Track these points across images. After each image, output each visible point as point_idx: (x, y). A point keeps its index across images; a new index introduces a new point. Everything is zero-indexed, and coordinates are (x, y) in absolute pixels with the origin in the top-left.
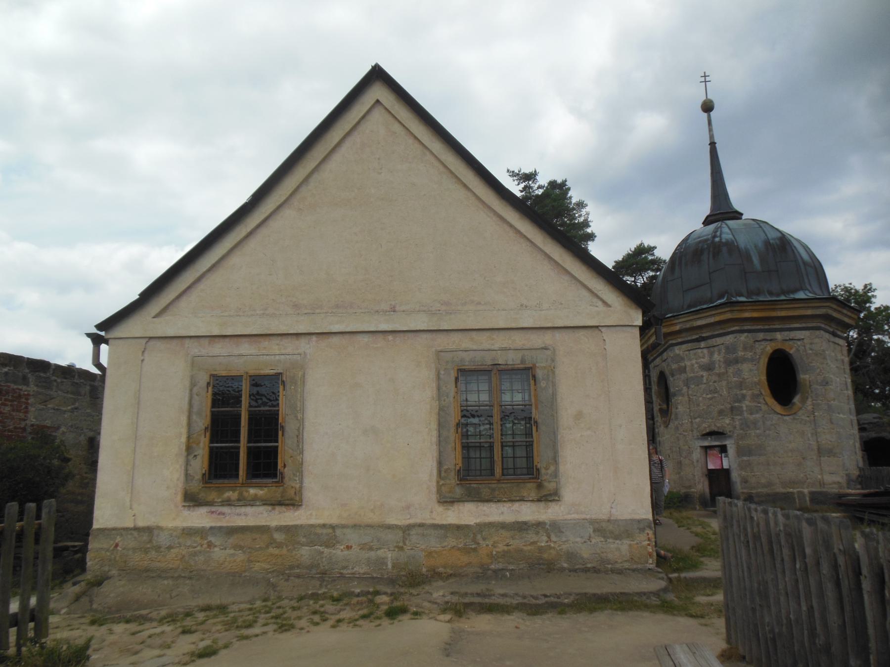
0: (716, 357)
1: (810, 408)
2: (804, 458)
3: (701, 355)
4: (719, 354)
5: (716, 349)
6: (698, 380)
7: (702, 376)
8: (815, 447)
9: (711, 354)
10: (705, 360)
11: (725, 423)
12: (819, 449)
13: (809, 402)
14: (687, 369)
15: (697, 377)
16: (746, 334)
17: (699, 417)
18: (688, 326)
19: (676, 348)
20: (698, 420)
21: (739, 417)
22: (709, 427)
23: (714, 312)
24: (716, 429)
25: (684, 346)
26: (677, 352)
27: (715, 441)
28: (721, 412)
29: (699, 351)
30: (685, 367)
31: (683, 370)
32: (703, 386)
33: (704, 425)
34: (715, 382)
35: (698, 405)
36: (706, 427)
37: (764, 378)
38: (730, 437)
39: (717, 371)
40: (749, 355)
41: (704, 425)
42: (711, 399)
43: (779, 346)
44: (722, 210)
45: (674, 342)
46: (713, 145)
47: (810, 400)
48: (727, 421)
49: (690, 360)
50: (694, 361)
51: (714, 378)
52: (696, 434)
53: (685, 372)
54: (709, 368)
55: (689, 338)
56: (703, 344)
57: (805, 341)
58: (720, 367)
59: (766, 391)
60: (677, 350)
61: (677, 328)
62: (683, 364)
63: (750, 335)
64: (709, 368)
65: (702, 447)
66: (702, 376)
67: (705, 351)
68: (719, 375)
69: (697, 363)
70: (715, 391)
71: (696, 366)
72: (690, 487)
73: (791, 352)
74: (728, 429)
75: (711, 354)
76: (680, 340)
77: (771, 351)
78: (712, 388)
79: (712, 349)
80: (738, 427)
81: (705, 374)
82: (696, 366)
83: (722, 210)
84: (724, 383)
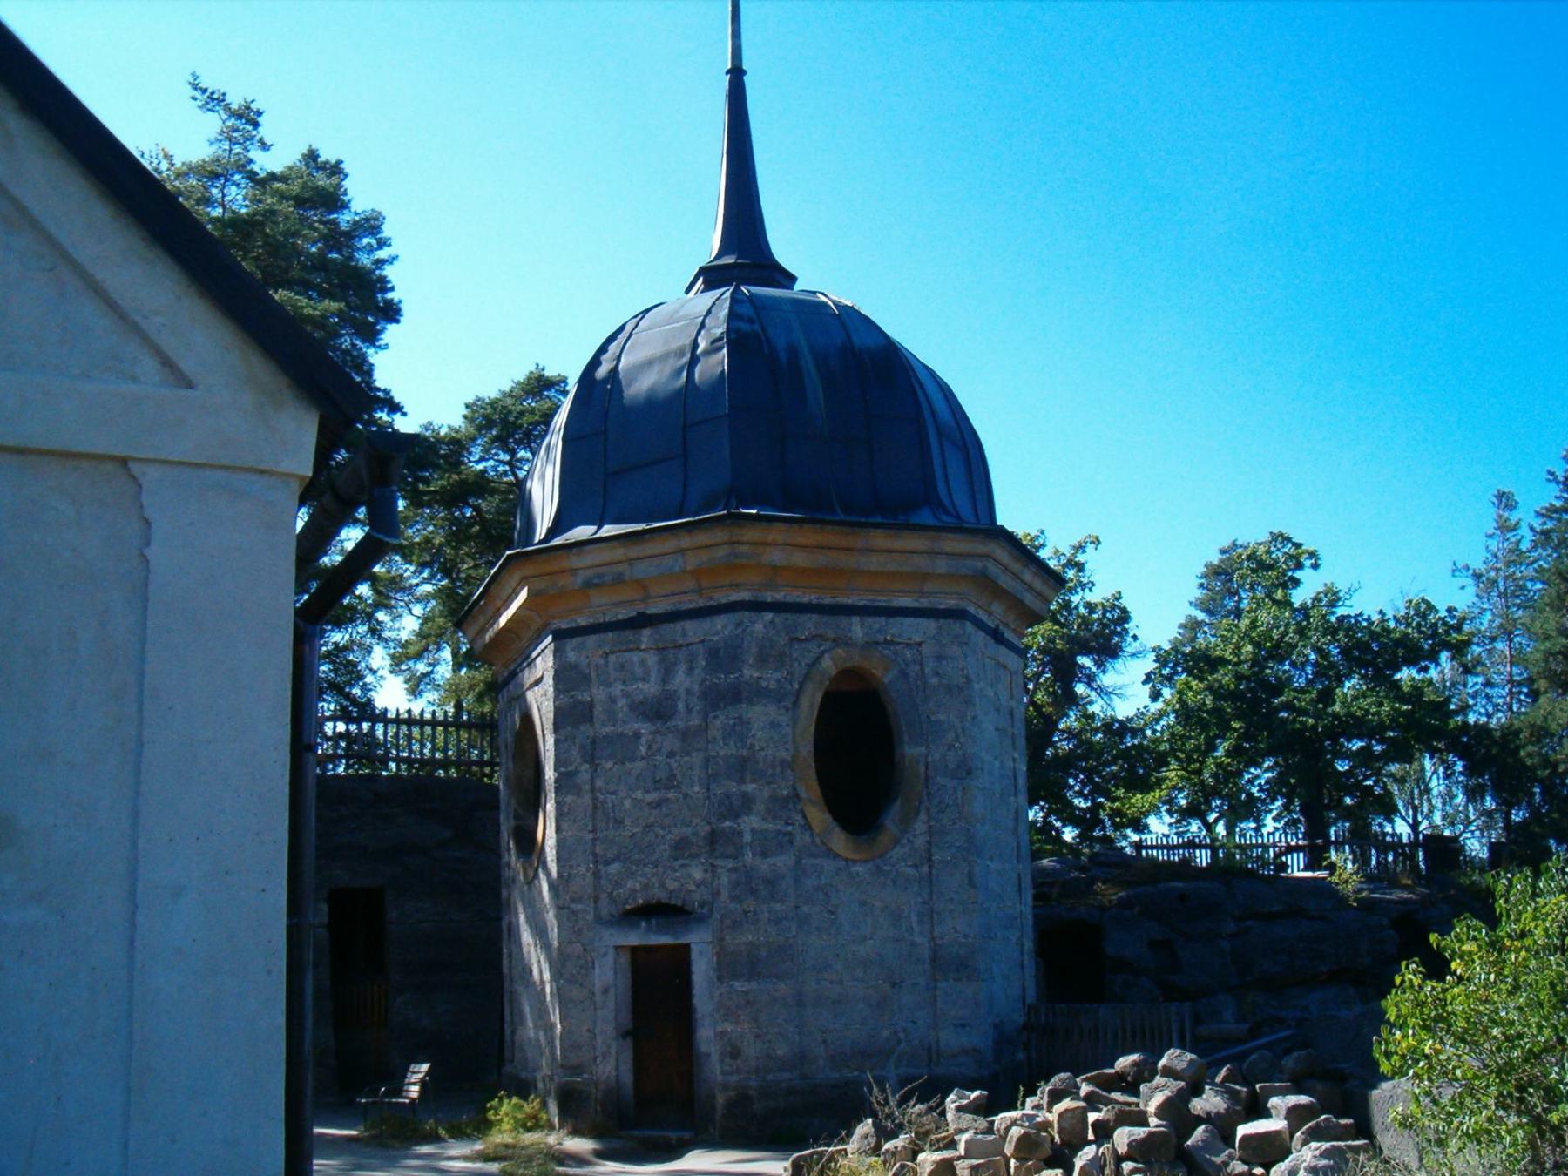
0: (681, 680)
1: (920, 842)
2: (893, 985)
3: (639, 671)
4: (691, 669)
5: (682, 654)
6: (624, 746)
7: (637, 735)
8: (926, 954)
9: (667, 672)
10: (651, 688)
11: (689, 879)
12: (934, 959)
13: (920, 826)
14: (598, 711)
15: (622, 735)
16: (769, 616)
17: (617, 858)
20: (615, 868)
21: (730, 864)
22: (646, 887)
24: (664, 897)
25: (592, 640)
27: (661, 931)
30: (591, 705)
32: (638, 766)
34: (671, 754)
35: (619, 823)
36: (638, 887)
37: (807, 749)
38: (702, 919)
40: (771, 678)
41: (630, 884)
42: (657, 805)
43: (857, 660)
44: (745, 255)
46: (737, 74)
47: (923, 816)
48: (698, 874)
49: (607, 684)
50: (618, 689)
51: (671, 742)
57: (925, 649)
58: (689, 710)
59: (810, 788)
63: (779, 619)
64: (658, 711)
66: (637, 735)
68: (685, 735)
69: (626, 695)
70: (670, 782)
71: (622, 702)
73: (887, 678)
75: (667, 672)
77: (833, 672)
81: (645, 728)
83: (745, 255)
84: (696, 759)
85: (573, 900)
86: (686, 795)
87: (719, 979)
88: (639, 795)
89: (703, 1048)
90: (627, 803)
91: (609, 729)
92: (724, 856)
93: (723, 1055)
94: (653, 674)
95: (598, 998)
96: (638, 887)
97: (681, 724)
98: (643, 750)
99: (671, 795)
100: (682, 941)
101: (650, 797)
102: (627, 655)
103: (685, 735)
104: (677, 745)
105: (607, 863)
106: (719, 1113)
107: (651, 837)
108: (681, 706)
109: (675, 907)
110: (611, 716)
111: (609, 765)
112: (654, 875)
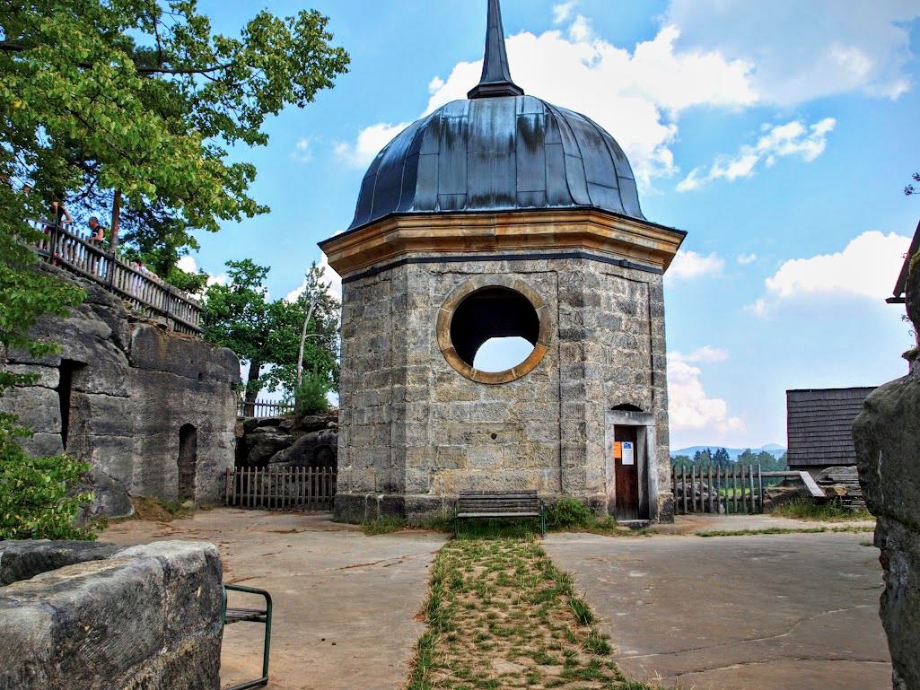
3: (621, 288)
5: (638, 284)
7: (620, 319)
9: (633, 291)
10: (625, 297)
17: (610, 379)
18: (627, 238)
19: (592, 263)
20: (611, 383)
21: (660, 390)
23: (663, 237)
24: (630, 401)
25: (602, 265)
26: (592, 269)
27: (633, 419)
28: (638, 378)
29: (619, 280)
31: (596, 301)
33: (617, 393)
34: (635, 332)
36: (622, 394)
39: (638, 317)
41: (617, 393)
42: (629, 355)
45: (588, 252)
51: (635, 327)
52: (607, 405)
53: (599, 305)
54: (629, 309)
55: (610, 256)
56: (626, 273)
60: (592, 268)
61: (613, 235)
62: (598, 292)
64: (629, 309)
65: (617, 427)
67: (626, 283)
68: (641, 324)
69: (615, 297)
71: (613, 300)
72: (595, 489)
74: (646, 404)
76: (596, 253)
78: (631, 341)
79: (634, 283)
80: (659, 404)
81: (624, 316)
82: (613, 300)
84: (646, 337)
85: (593, 398)
86: (641, 353)
87: (657, 443)
88: (620, 348)
89: (652, 477)
90: (615, 352)
91: (607, 312)
92: (658, 386)
93: (659, 480)
94: (627, 290)
95: (607, 451)
96: (620, 395)
97: (640, 319)
98: (623, 328)
99: (635, 352)
100: (643, 424)
101: (626, 351)
102: (615, 278)
103: (641, 324)
104: (638, 328)
105: (607, 381)
106: (659, 510)
107: (626, 371)
108: (638, 310)
109: (636, 407)
110: (609, 307)
111: (607, 330)
112: (628, 390)
